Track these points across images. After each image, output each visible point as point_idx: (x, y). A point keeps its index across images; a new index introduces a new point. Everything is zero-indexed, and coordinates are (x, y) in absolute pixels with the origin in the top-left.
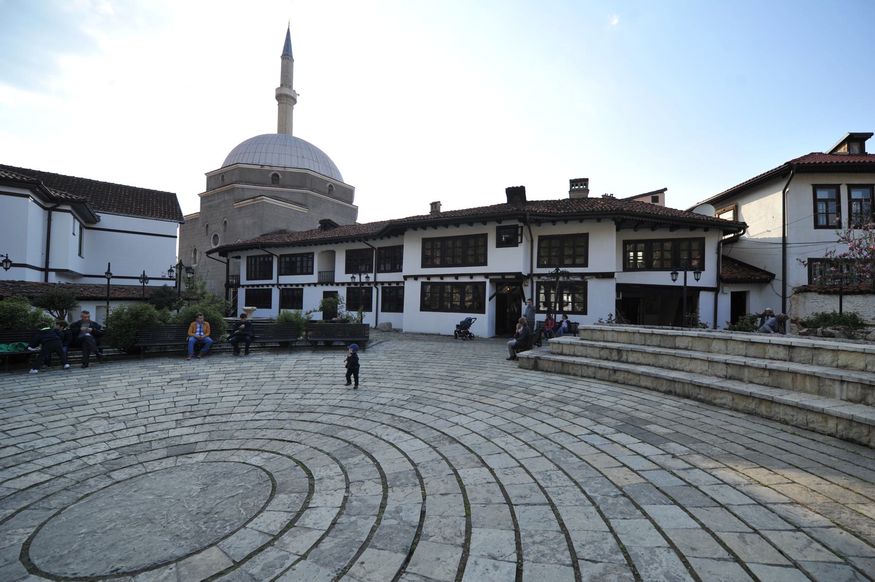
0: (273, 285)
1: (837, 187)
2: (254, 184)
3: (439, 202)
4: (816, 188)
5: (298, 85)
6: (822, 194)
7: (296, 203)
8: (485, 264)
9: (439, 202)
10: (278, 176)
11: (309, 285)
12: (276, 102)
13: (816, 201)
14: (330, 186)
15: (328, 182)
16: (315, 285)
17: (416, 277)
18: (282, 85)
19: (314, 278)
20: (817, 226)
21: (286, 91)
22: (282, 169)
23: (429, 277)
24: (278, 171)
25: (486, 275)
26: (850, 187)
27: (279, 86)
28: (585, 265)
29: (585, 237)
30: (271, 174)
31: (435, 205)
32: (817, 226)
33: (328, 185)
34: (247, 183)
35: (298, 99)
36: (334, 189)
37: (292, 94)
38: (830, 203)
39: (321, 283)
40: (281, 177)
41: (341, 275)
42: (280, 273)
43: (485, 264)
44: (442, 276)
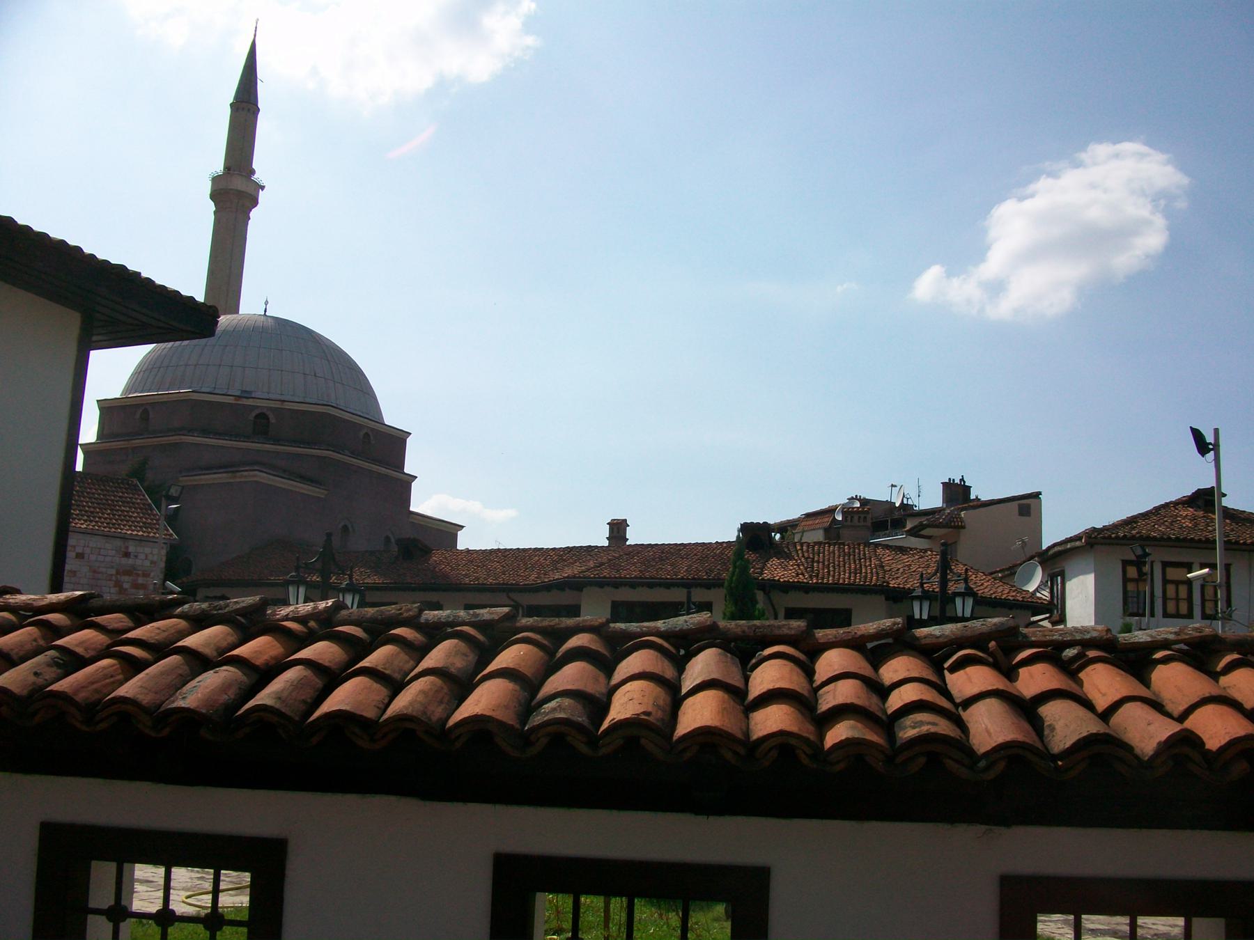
2: (218, 434)
3: (626, 520)
5: (263, 164)
7: (303, 478)
9: (626, 520)
10: (268, 419)
12: (211, 207)
13: (1126, 581)
14: (367, 435)
15: (361, 426)
18: (228, 168)
21: (238, 184)
22: (278, 405)
24: (270, 409)
26: (1165, 565)
27: (219, 167)
30: (254, 414)
31: (618, 528)
33: (362, 433)
34: (205, 432)
35: (262, 196)
36: (373, 442)
37: (250, 190)
38: (1168, 577)
40: (273, 420)
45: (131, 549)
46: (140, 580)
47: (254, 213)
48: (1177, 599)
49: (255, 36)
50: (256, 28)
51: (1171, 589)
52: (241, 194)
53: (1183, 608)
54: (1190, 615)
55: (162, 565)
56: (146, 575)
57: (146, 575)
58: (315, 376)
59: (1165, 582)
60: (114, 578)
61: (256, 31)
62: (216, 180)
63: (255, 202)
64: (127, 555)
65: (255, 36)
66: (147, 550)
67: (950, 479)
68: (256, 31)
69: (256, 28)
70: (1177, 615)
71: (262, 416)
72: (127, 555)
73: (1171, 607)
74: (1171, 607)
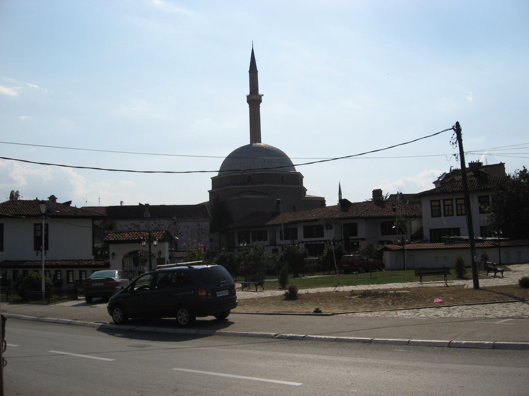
0: (251, 247)
1: (439, 201)
4: (431, 201)
6: (434, 204)
8: (323, 236)
10: (251, 177)
11: (267, 246)
12: (247, 105)
13: (432, 206)
14: (282, 176)
16: (269, 246)
17: (303, 242)
19: (267, 243)
20: (432, 217)
21: (254, 97)
23: (307, 242)
25: (325, 241)
27: (248, 93)
28: (356, 235)
29: (357, 224)
32: (432, 217)
39: (271, 245)
41: (279, 241)
42: (254, 240)
43: (323, 236)
44: (315, 241)
45: (201, 224)
46: (204, 231)
47: (261, 105)
48: (448, 210)
49: (253, 47)
50: (253, 44)
51: (459, 207)
52: (255, 100)
53: (451, 213)
54: (453, 215)
55: (209, 227)
56: (205, 230)
57: (205, 230)
58: (265, 161)
59: (457, 205)
60: (197, 232)
61: (253, 45)
62: (248, 97)
63: (261, 101)
64: (199, 225)
65: (253, 47)
66: (205, 224)
67: (471, 162)
68: (253, 45)
69: (253, 44)
70: (449, 216)
71: (249, 177)
72: (199, 225)
73: (459, 212)
74: (447, 213)
